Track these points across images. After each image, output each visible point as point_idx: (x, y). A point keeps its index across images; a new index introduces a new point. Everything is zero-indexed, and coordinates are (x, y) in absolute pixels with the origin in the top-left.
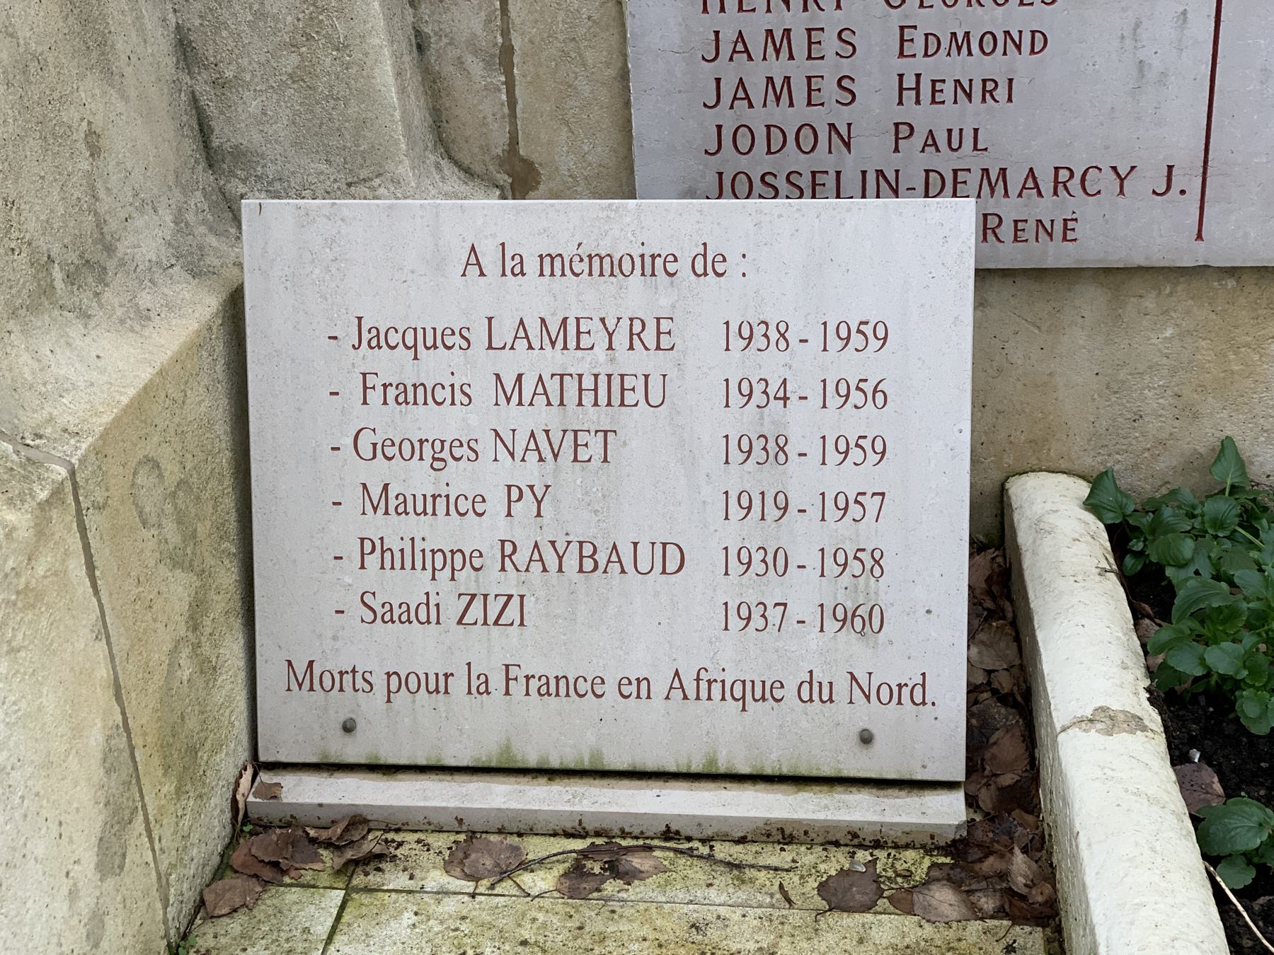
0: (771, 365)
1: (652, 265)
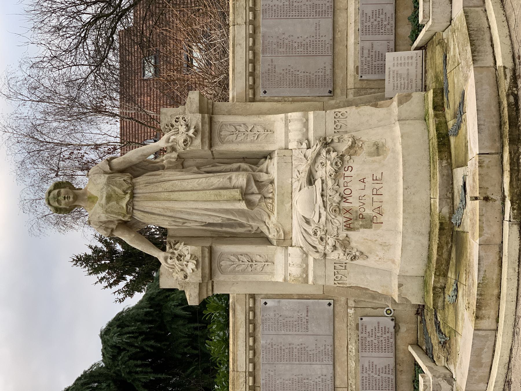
0: (396, 64)
1: (389, 72)
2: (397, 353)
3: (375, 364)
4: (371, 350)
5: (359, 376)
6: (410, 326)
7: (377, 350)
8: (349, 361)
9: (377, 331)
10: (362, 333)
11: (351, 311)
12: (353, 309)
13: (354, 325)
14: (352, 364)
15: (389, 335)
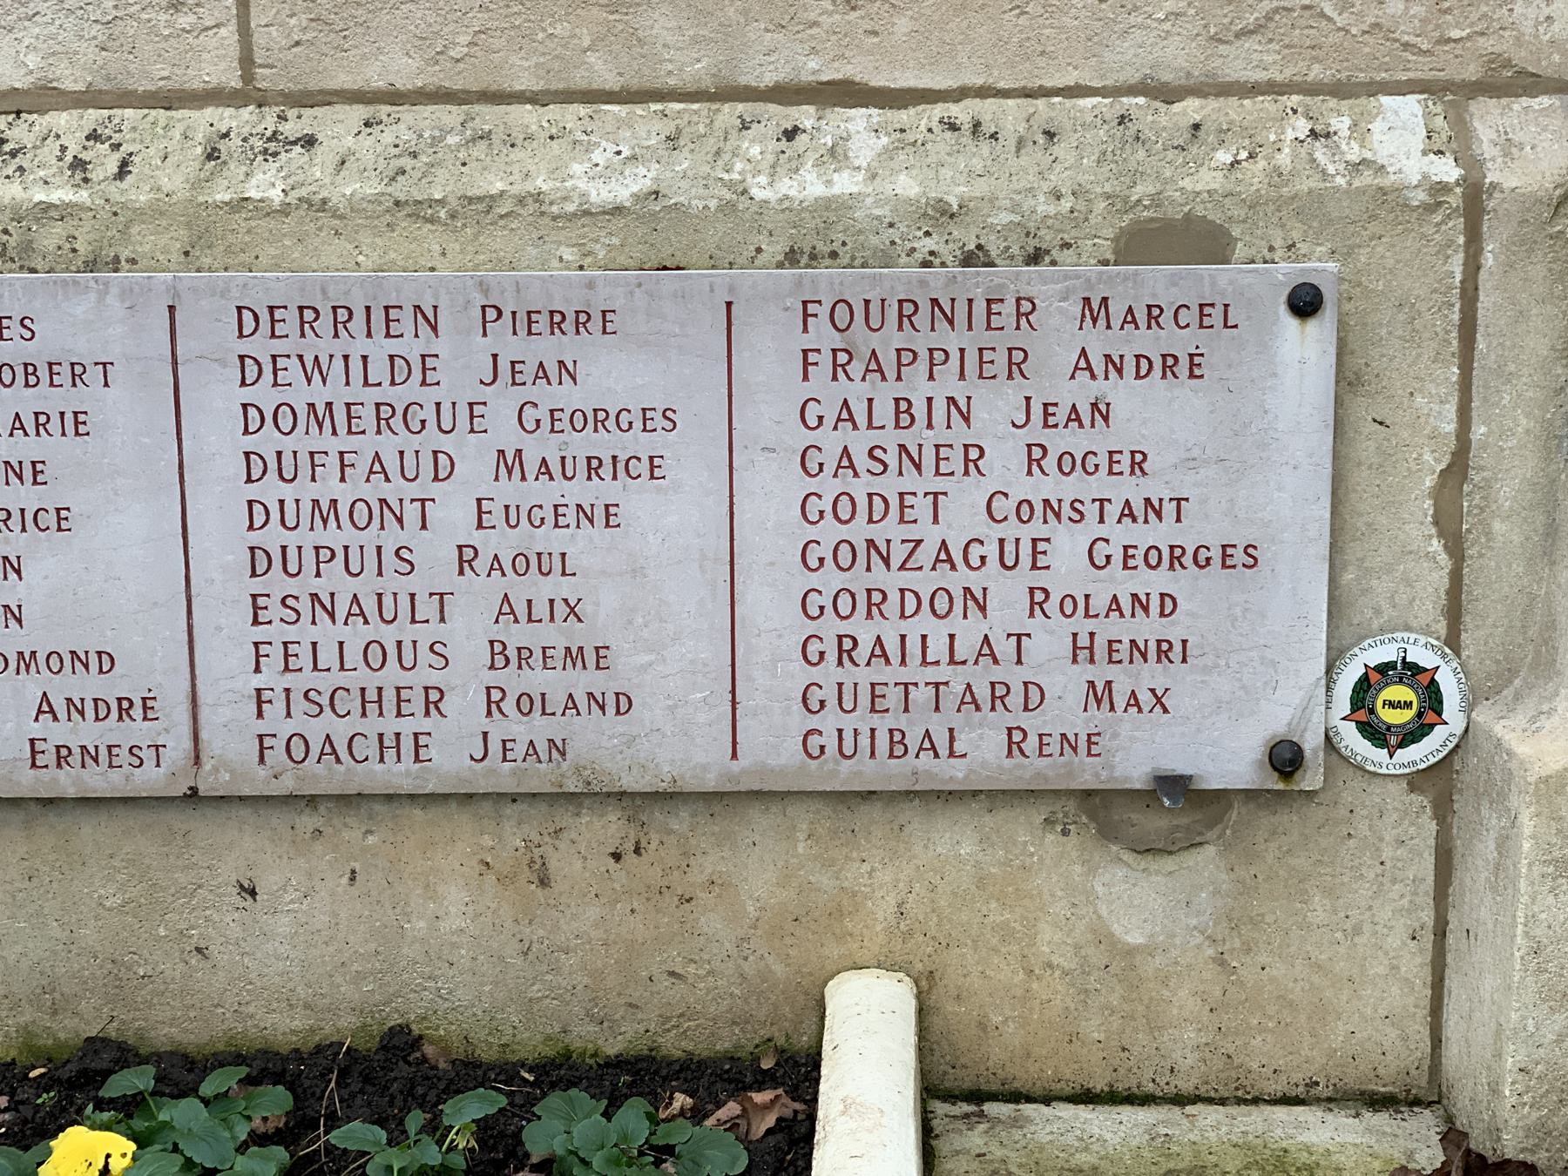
2: (802, 816)
3: (635, 499)
4: (831, 442)
5: (437, 268)
6: (1184, 1000)
7: (830, 533)
8: (648, 124)
9: (1121, 534)
10: (1094, 311)
11: (1400, 140)
12: (1447, 170)
13: (1202, 180)
14: (604, 165)
15: (1065, 710)
